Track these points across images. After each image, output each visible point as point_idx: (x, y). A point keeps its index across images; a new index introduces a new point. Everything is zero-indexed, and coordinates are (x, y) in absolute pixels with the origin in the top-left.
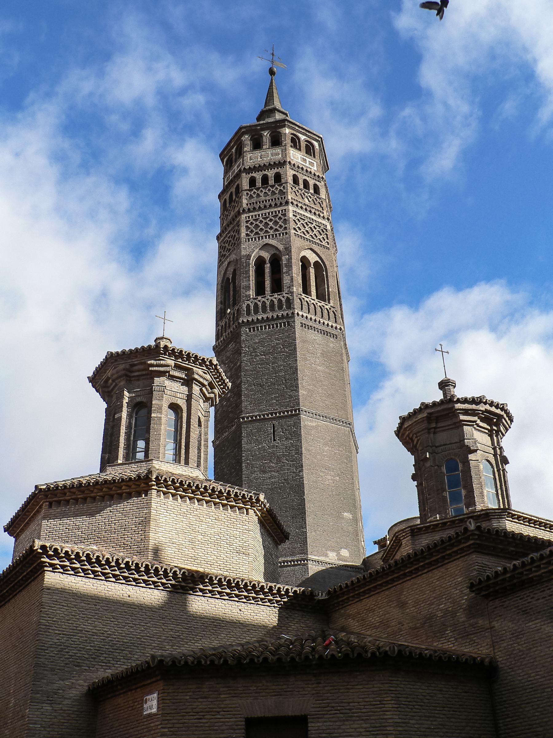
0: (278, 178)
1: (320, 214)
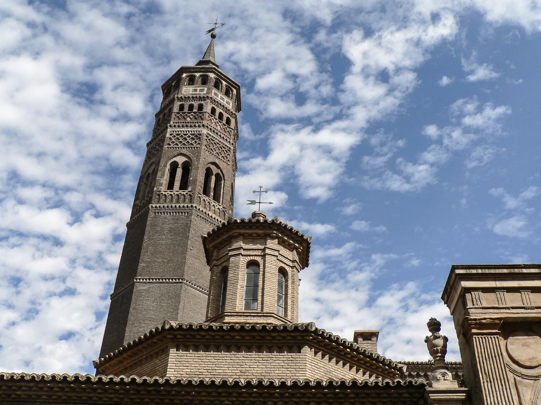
0: (201, 107)
1: (227, 139)
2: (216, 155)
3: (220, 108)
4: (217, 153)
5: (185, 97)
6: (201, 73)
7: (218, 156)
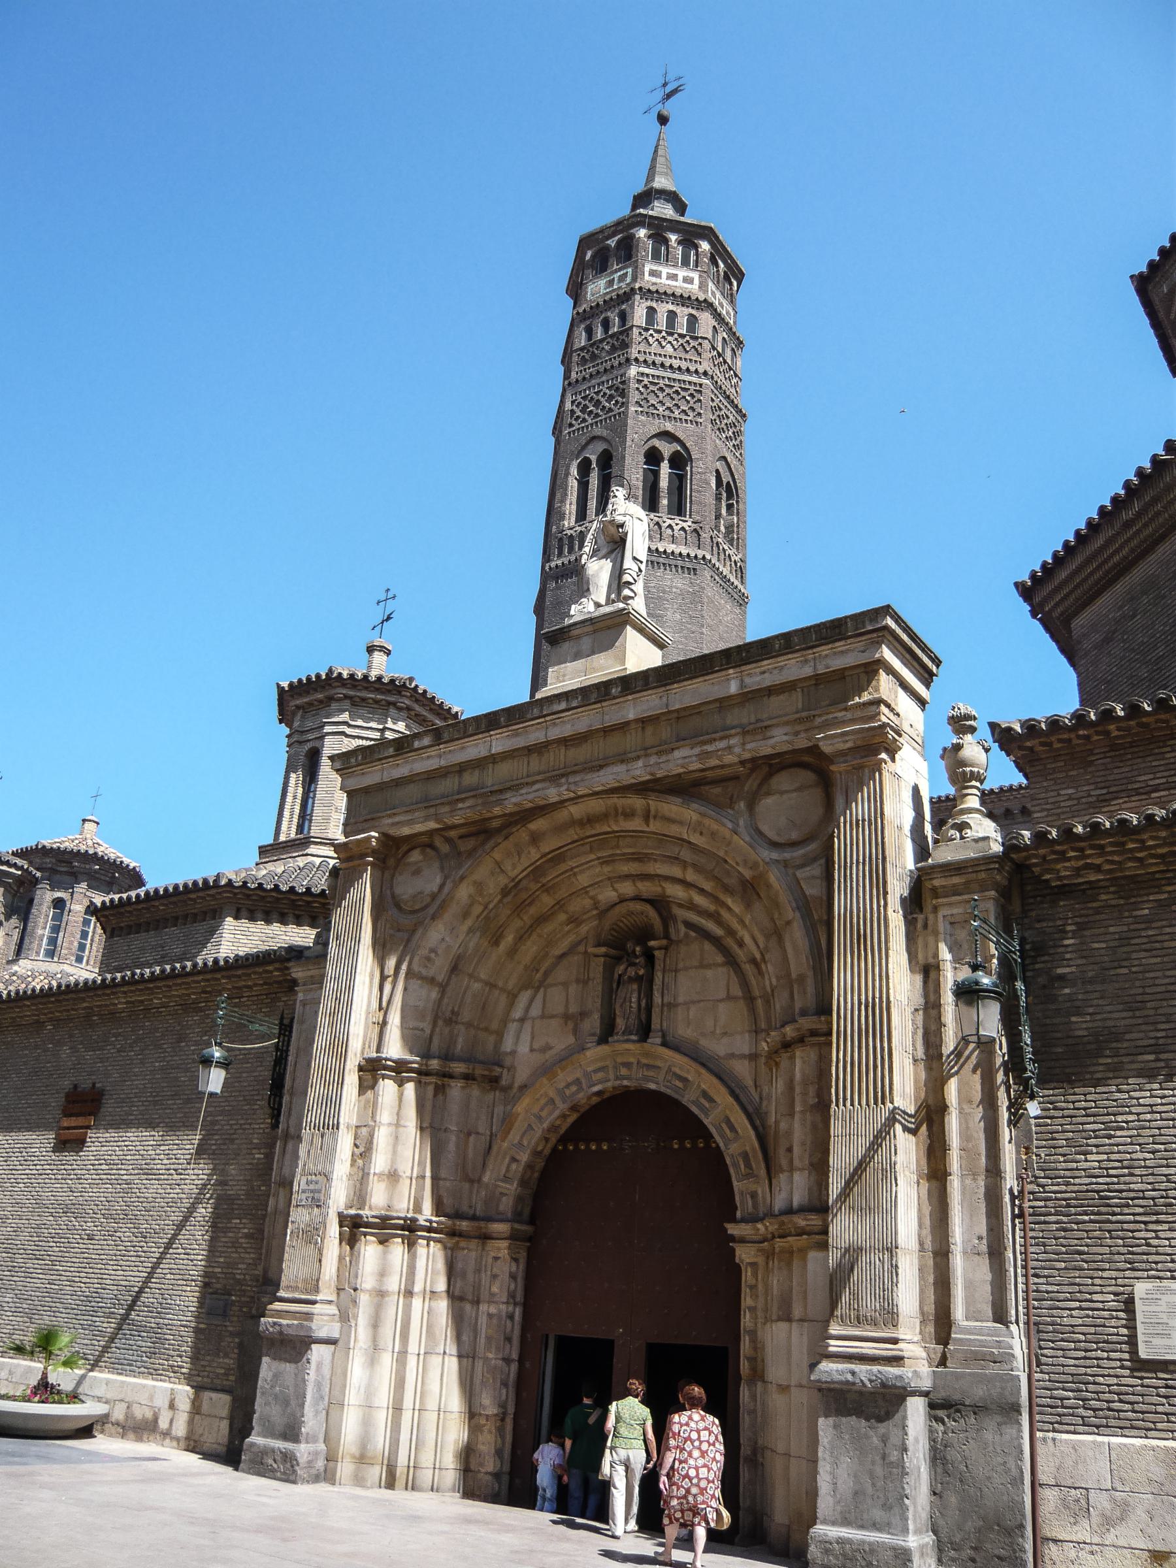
2: (667, 413)
3: (667, 303)
4: (668, 408)
5: (591, 307)
6: (619, 236)
7: (672, 415)
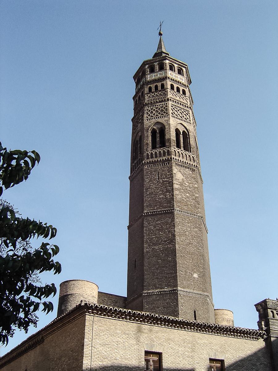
0: (163, 86)
2: (180, 118)
